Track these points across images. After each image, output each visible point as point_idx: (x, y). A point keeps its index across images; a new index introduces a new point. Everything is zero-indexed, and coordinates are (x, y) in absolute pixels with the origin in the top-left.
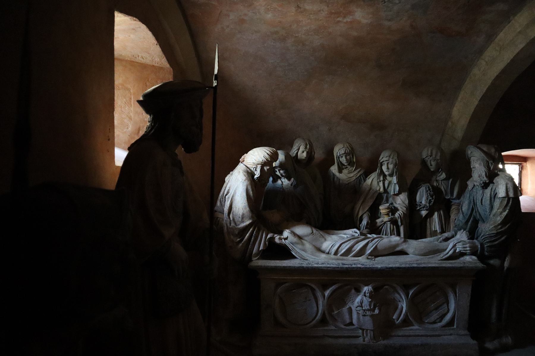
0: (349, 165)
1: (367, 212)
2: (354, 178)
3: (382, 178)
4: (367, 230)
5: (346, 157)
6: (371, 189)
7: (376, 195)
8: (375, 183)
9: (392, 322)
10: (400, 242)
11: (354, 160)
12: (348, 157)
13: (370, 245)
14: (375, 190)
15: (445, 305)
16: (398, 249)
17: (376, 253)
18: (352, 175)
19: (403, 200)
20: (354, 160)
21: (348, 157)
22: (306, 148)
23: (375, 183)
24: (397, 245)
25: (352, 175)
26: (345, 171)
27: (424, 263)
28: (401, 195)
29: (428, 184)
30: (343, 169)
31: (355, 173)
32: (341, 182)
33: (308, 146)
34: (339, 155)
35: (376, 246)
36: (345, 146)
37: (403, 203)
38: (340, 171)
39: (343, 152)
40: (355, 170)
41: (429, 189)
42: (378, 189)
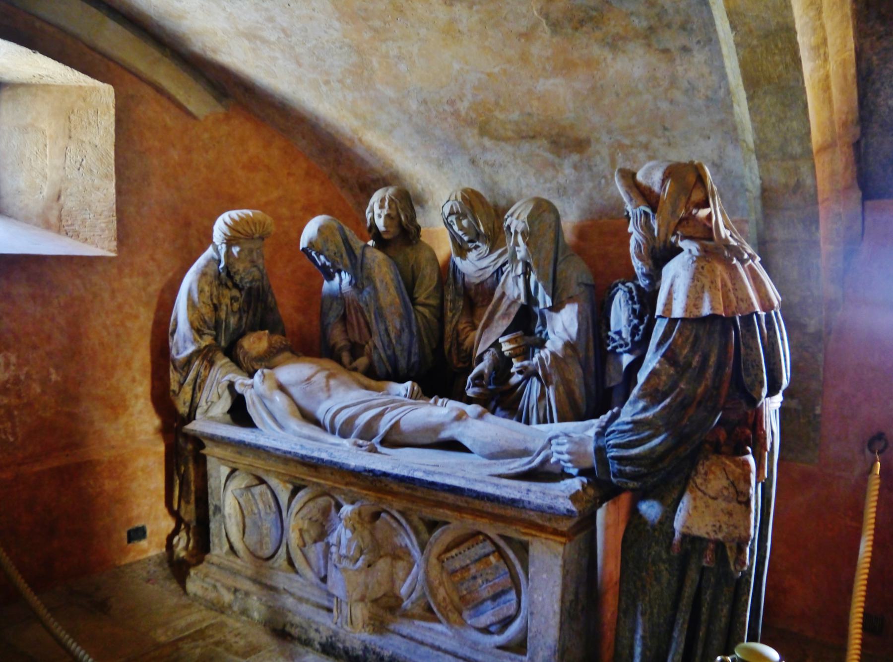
1: (492, 350)
2: (491, 270)
3: (520, 270)
4: (476, 390)
5: (459, 220)
6: (503, 295)
7: (515, 310)
8: (510, 280)
9: (399, 600)
10: (447, 419)
11: (482, 228)
12: (465, 223)
13: (387, 417)
14: (511, 297)
15: (512, 595)
16: (445, 435)
17: (394, 440)
18: (485, 263)
19: (567, 324)
20: (482, 228)
21: (465, 223)
22: (381, 207)
23: (510, 280)
24: (441, 426)
25: (485, 263)
26: (472, 255)
27: (440, 474)
28: (563, 311)
29: (630, 284)
30: (470, 250)
32: (466, 279)
33: (386, 204)
35: (397, 422)
37: (565, 330)
40: (491, 252)
41: (632, 298)
42: (516, 296)
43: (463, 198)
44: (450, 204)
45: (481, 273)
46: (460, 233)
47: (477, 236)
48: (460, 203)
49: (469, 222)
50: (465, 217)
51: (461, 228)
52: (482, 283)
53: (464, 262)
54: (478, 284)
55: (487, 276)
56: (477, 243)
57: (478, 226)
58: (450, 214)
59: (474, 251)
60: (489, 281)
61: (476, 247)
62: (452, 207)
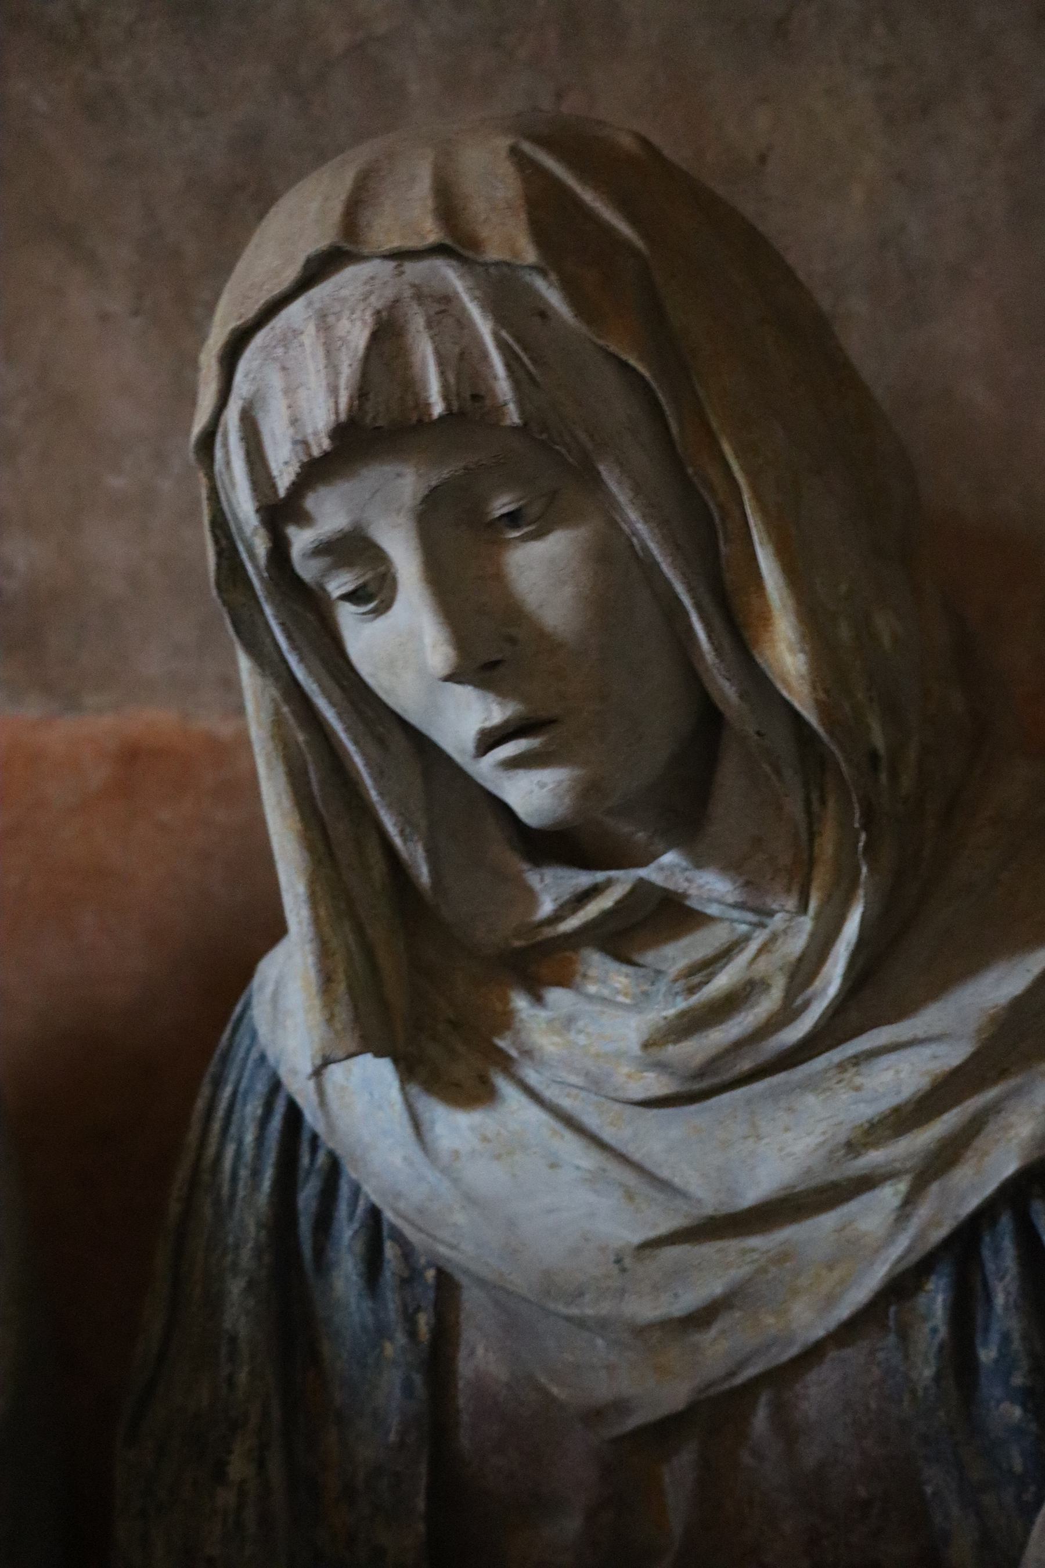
0: (684, 812)
2: (877, 1235)
11: (787, 656)
12: (543, 571)
18: (782, 1140)
20: (787, 656)
21: (543, 571)
25: (782, 1140)
26: (592, 1028)
30: (542, 962)
31: (901, 1065)
32: (480, 1357)
34: (244, 506)
36: (407, 214)
38: (436, 1005)
39: (320, 416)
40: (876, 993)
43: (550, 214)
44: (352, 298)
45: (714, 1271)
46: (459, 719)
47: (686, 767)
48: (504, 294)
49: (614, 562)
50: (554, 473)
51: (489, 645)
52: (718, 1413)
53: (453, 1126)
54: (665, 1431)
55: (808, 1321)
56: (668, 868)
57: (739, 628)
58: (354, 443)
59: (605, 975)
60: (817, 1393)
61: (651, 920)
62: (387, 333)
